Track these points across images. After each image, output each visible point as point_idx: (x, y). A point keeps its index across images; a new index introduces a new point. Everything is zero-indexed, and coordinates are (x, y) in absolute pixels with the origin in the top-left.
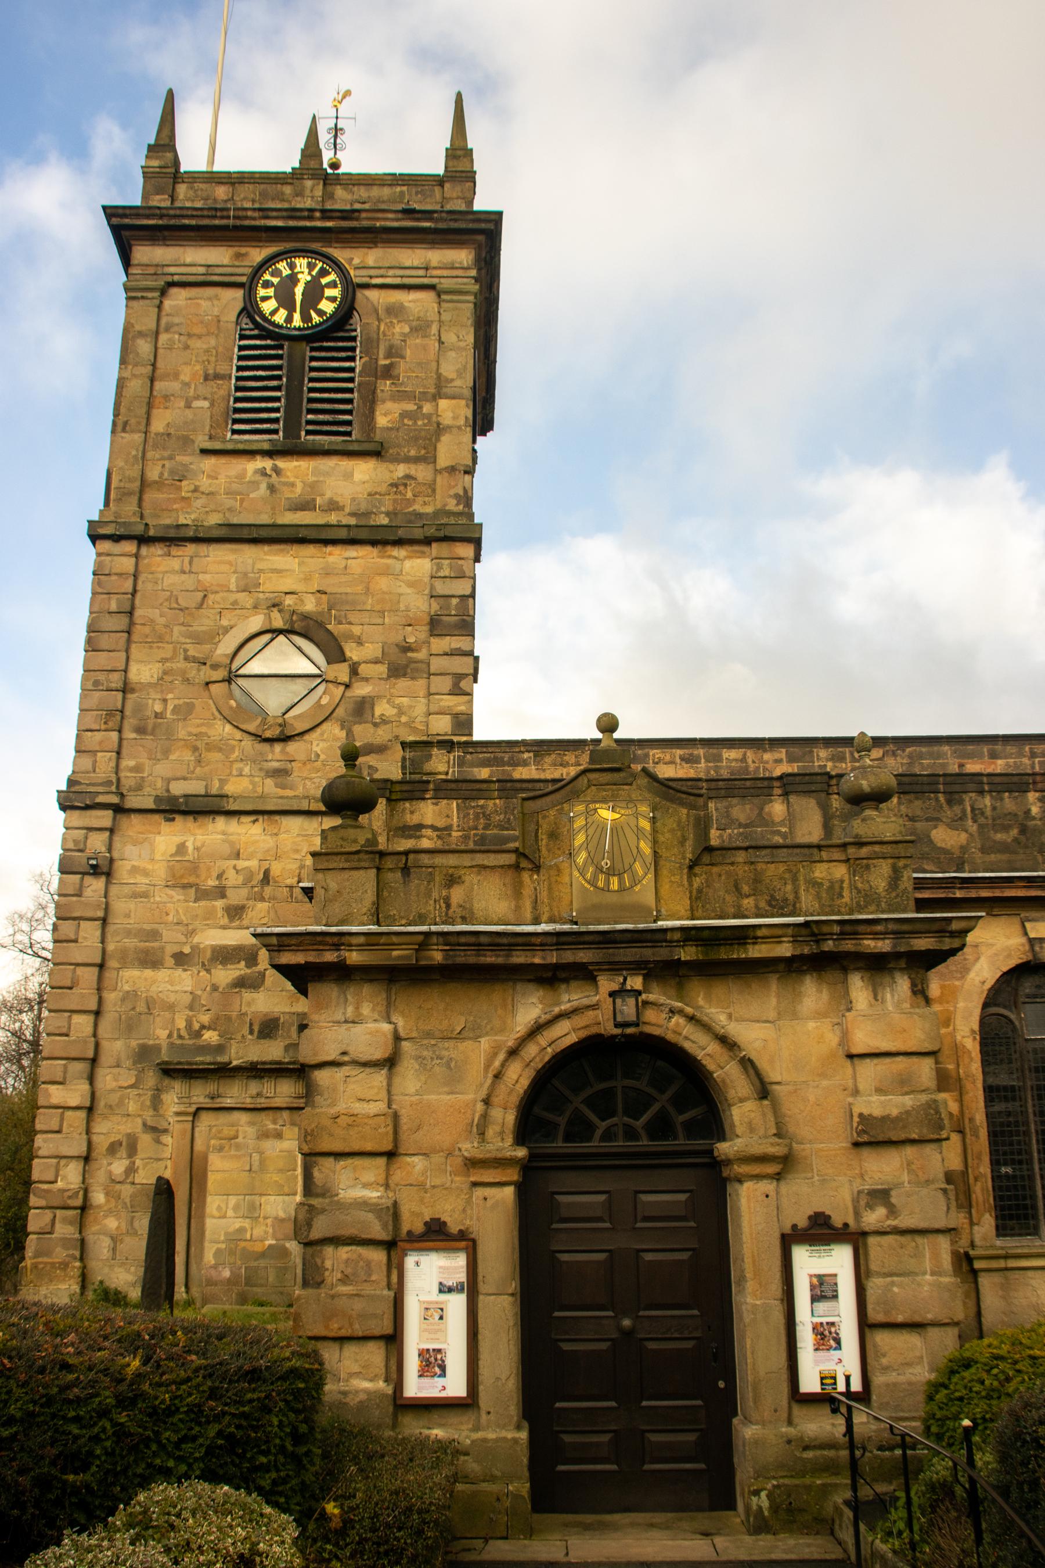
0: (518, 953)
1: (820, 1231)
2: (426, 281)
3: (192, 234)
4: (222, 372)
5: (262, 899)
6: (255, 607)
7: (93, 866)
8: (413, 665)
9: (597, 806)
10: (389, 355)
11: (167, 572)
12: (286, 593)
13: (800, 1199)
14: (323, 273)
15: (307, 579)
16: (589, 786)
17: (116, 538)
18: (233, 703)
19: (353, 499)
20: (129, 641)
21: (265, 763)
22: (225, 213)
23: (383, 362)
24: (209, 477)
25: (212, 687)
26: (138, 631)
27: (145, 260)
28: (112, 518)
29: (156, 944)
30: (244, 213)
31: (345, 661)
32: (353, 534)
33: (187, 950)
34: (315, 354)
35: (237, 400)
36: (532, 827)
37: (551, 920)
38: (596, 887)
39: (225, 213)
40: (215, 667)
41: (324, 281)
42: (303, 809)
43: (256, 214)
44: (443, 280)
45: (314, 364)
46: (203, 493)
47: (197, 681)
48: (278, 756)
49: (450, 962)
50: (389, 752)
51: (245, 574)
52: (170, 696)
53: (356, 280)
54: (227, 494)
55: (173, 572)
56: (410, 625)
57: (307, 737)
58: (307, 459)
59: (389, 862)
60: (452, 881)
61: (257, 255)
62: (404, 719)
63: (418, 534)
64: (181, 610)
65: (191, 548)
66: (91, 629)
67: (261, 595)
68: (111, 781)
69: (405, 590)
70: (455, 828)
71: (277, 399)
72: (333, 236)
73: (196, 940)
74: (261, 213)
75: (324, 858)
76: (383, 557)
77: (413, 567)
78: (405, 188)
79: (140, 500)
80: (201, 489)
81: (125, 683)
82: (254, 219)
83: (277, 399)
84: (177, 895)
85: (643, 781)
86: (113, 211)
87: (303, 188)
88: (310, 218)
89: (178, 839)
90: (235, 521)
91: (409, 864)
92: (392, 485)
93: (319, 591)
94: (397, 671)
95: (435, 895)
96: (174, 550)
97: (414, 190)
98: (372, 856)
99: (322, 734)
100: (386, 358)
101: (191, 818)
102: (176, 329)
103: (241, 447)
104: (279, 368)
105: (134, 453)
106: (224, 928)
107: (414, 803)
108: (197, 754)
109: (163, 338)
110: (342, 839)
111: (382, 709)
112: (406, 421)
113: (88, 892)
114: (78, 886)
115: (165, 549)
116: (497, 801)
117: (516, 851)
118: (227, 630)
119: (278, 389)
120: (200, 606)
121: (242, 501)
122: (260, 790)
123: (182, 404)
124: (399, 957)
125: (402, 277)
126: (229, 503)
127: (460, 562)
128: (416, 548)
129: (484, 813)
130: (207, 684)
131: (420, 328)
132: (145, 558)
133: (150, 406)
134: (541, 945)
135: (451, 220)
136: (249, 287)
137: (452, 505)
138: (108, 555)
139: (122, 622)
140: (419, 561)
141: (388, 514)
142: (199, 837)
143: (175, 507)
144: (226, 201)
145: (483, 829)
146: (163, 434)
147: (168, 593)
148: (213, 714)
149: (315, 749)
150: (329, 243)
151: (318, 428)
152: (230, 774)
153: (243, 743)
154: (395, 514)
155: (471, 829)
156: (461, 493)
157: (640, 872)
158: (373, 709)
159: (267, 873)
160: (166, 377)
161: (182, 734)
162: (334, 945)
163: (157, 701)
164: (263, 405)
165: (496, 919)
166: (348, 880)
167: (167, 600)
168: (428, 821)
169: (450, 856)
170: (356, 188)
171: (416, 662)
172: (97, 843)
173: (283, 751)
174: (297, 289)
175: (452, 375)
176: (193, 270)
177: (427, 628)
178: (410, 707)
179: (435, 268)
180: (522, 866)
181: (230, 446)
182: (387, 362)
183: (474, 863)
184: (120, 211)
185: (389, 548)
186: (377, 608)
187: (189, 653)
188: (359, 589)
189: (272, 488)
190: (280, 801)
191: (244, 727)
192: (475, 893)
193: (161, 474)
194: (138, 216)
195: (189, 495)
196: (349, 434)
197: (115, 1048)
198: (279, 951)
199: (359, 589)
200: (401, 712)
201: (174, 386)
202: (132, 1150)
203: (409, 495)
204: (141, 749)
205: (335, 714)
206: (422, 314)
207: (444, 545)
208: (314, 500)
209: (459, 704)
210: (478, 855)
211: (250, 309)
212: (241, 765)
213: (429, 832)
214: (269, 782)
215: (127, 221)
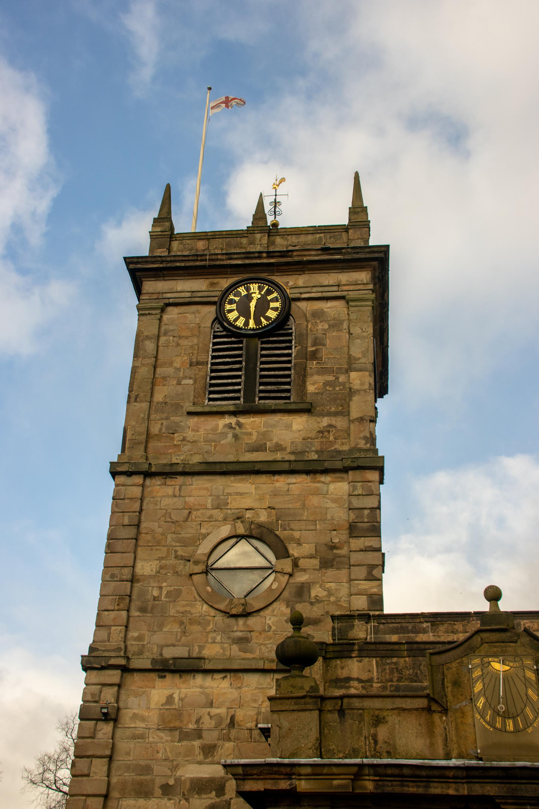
0: (435, 784)
2: (338, 294)
3: (182, 272)
4: (202, 360)
5: (229, 740)
6: (225, 520)
7: (104, 714)
8: (337, 559)
9: (490, 659)
10: (315, 344)
11: (163, 496)
12: (247, 509)
14: (269, 292)
15: (261, 499)
16: (482, 644)
17: (129, 474)
18: (209, 589)
19: (293, 443)
20: (136, 546)
21: (232, 633)
22: (203, 258)
23: (310, 349)
24: (193, 430)
25: (195, 577)
26: (144, 538)
27: (151, 290)
28: (127, 460)
29: (148, 777)
30: (216, 257)
31: (289, 557)
32: (293, 467)
33: (171, 782)
34: (264, 346)
35: (212, 378)
36: (439, 677)
37: (460, 756)
38: (495, 728)
39: (203, 258)
40: (196, 563)
41: (269, 298)
42: (259, 668)
43: (224, 257)
44: (350, 293)
45: (264, 352)
46: (189, 441)
47: (183, 573)
48: (241, 628)
49: (379, 791)
50: (322, 624)
51: (218, 497)
52: (164, 584)
53: (291, 296)
54: (205, 442)
55: (168, 496)
56: (335, 530)
57: (262, 613)
58: (260, 416)
59: (328, 705)
60: (378, 721)
61: (225, 283)
62: (332, 599)
63: (339, 465)
64: (173, 522)
65: (180, 480)
66: (111, 537)
67: (229, 511)
68: (121, 648)
69: (330, 505)
70: (376, 680)
71: (239, 377)
72: (275, 268)
73: (179, 773)
74: (227, 256)
75: (278, 701)
76: (314, 482)
77: (335, 489)
78: (322, 235)
79: (146, 447)
80: (188, 439)
81: (133, 575)
82: (223, 260)
83: (239, 377)
84: (165, 736)
85: (526, 639)
86: (131, 260)
87: (255, 239)
88: (259, 258)
89: (167, 692)
90: (211, 460)
91: (344, 707)
92: (319, 432)
93: (269, 507)
94: (326, 564)
95: (365, 732)
96: (169, 481)
97: (328, 236)
98: (314, 700)
99: (273, 611)
100: (313, 346)
101: (177, 675)
102: (171, 333)
103: (214, 409)
104: (240, 356)
105: (142, 416)
106: (200, 763)
107: (344, 660)
108: (183, 627)
109: (163, 339)
110: (292, 686)
111: (316, 592)
112: (328, 388)
113: (100, 735)
114: (92, 730)
115: (163, 481)
116: (407, 659)
117: (427, 696)
118: (205, 536)
119: (239, 370)
120: (186, 520)
121: (215, 446)
122: (228, 653)
123: (175, 382)
124: (339, 786)
125: (322, 292)
126: (206, 448)
127: (369, 484)
128: (338, 475)
129: (397, 669)
130: (191, 575)
131: (336, 325)
132: (148, 487)
133: (153, 384)
134: (454, 777)
135: (354, 253)
136: (219, 304)
137: (362, 444)
138: (124, 485)
139: (132, 532)
140: (340, 484)
141: (317, 452)
142: (183, 690)
143: (169, 451)
144: (204, 250)
145: (397, 681)
146: (162, 403)
147: (164, 511)
148: (195, 597)
149: (268, 622)
150: (272, 273)
151: (267, 395)
152: (207, 642)
153: (216, 618)
154: (322, 452)
155: (388, 681)
156: (368, 436)
157: (531, 717)
158: (309, 592)
159: (233, 718)
160: (164, 365)
161: (172, 612)
162: (286, 774)
163: (155, 588)
164: (230, 381)
165: (414, 754)
166: (297, 720)
167: (163, 516)
168: (355, 675)
169: (376, 700)
170: (289, 237)
171: (340, 557)
172: (108, 695)
173: (245, 624)
174: (251, 304)
175: (359, 355)
176: (183, 295)
177: (347, 532)
178: (337, 590)
179: (344, 285)
180: (433, 708)
181: (207, 409)
182: (314, 349)
183: (395, 706)
184: (135, 260)
185: (318, 476)
186: (311, 518)
187: (178, 553)
188: (298, 505)
189: (236, 437)
190: (243, 662)
191: (216, 606)
192: (397, 731)
193: (161, 429)
194: (147, 262)
195: (180, 443)
196: (289, 398)
198: (244, 779)
199: (298, 505)
200: (330, 593)
201: (170, 371)
203: (332, 438)
204: (143, 623)
205: (282, 596)
206: (336, 316)
207: (357, 472)
208: (265, 444)
209: (372, 587)
210: (398, 700)
211: (220, 318)
212: (214, 635)
213: (355, 684)
214: (235, 647)
215: (139, 266)
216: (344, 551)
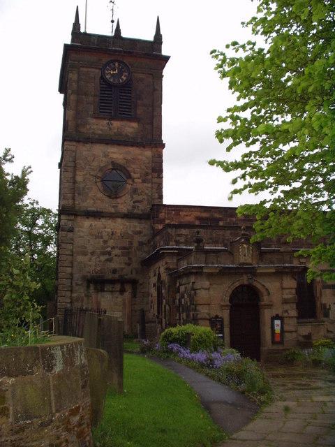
1: (277, 317)
13: (274, 312)
14: (123, 68)
197: (77, 276)
202: (82, 301)
216: (150, 177)
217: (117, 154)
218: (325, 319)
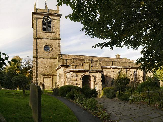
14: (49, 18)
65: (40, 39)
94: (55, 49)
161: (41, 52)
217: (48, 41)
218: (107, 84)
